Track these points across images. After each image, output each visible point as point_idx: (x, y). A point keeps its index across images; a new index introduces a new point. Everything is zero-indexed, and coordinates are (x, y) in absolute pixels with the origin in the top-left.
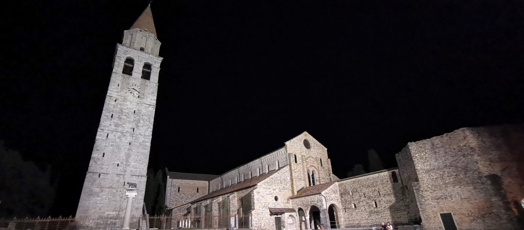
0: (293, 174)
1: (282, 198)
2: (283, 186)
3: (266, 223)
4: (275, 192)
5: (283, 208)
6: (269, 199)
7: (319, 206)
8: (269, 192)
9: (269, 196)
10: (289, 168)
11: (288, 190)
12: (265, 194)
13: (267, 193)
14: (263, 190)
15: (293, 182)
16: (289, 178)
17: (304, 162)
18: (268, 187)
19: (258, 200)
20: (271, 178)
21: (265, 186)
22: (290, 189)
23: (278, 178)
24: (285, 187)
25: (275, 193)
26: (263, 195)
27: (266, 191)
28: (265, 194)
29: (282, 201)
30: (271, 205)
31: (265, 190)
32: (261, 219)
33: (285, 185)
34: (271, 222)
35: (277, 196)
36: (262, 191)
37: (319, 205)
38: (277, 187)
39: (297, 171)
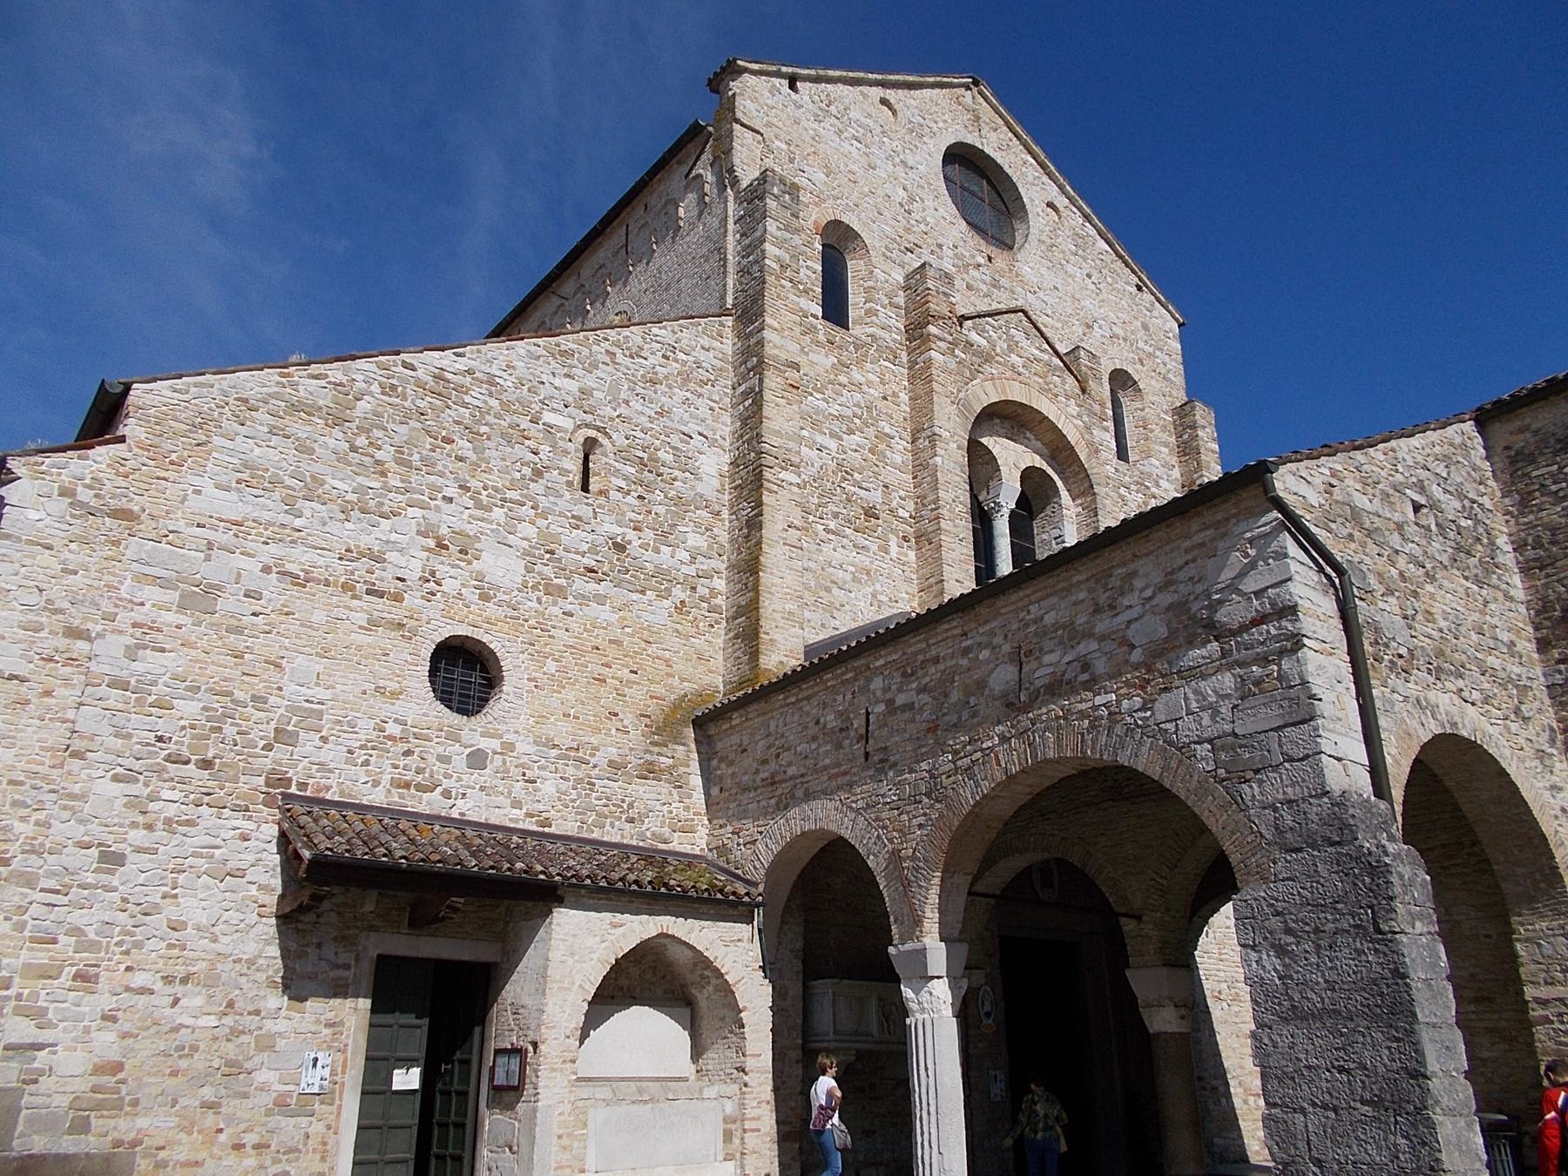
0: (779, 418)
1: (560, 682)
2: (609, 527)
3: (147, 1046)
4: (453, 579)
5: (566, 825)
6: (324, 653)
7: (1203, 750)
8: (347, 555)
9: (317, 607)
10: (729, 345)
11: (681, 607)
12: (252, 566)
13: (299, 559)
14: (232, 505)
15: (760, 504)
16: (714, 465)
17: (932, 329)
18: (341, 484)
19: (74, 633)
20: (420, 373)
21: (272, 455)
22: (720, 601)
23: (548, 417)
24: (634, 548)
25: (449, 586)
26: (211, 571)
27: (295, 537)
28: (252, 566)
29: (562, 732)
30: (332, 754)
31: (270, 509)
32: (48, 973)
33: (649, 535)
34: (267, 1044)
35: (494, 642)
36: (194, 502)
37: (1188, 729)
38: (498, 514)
39: (834, 409)
